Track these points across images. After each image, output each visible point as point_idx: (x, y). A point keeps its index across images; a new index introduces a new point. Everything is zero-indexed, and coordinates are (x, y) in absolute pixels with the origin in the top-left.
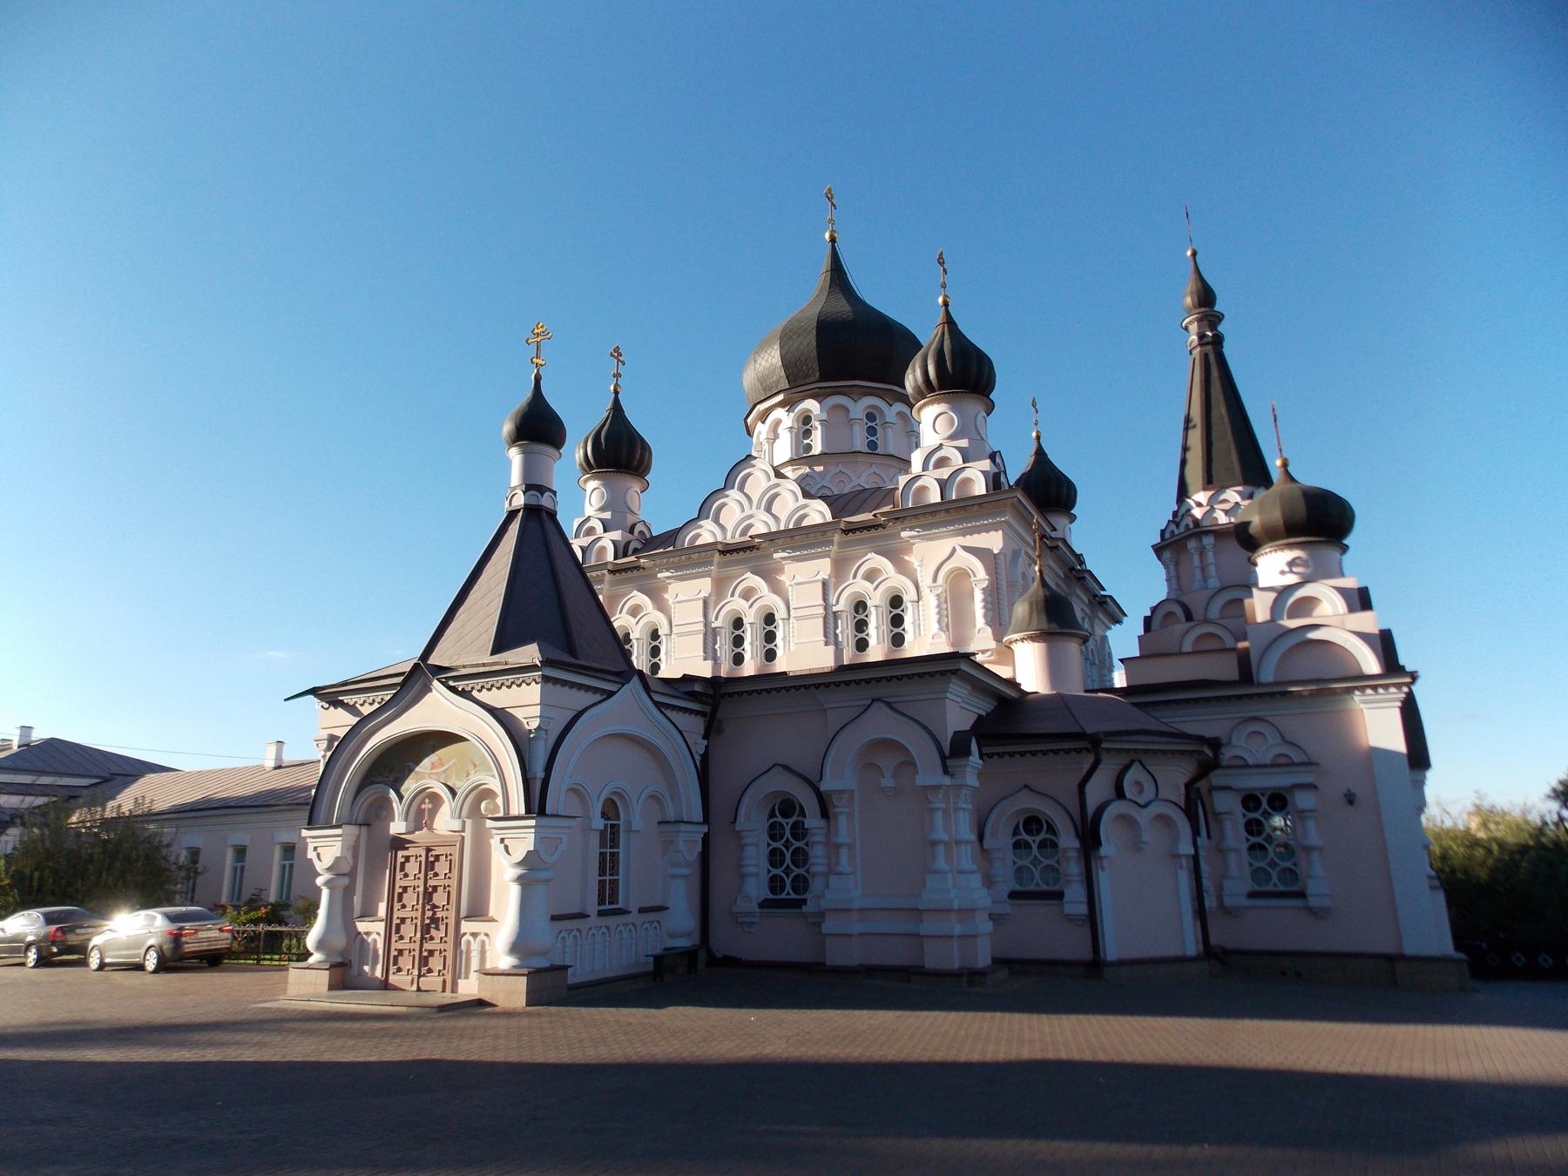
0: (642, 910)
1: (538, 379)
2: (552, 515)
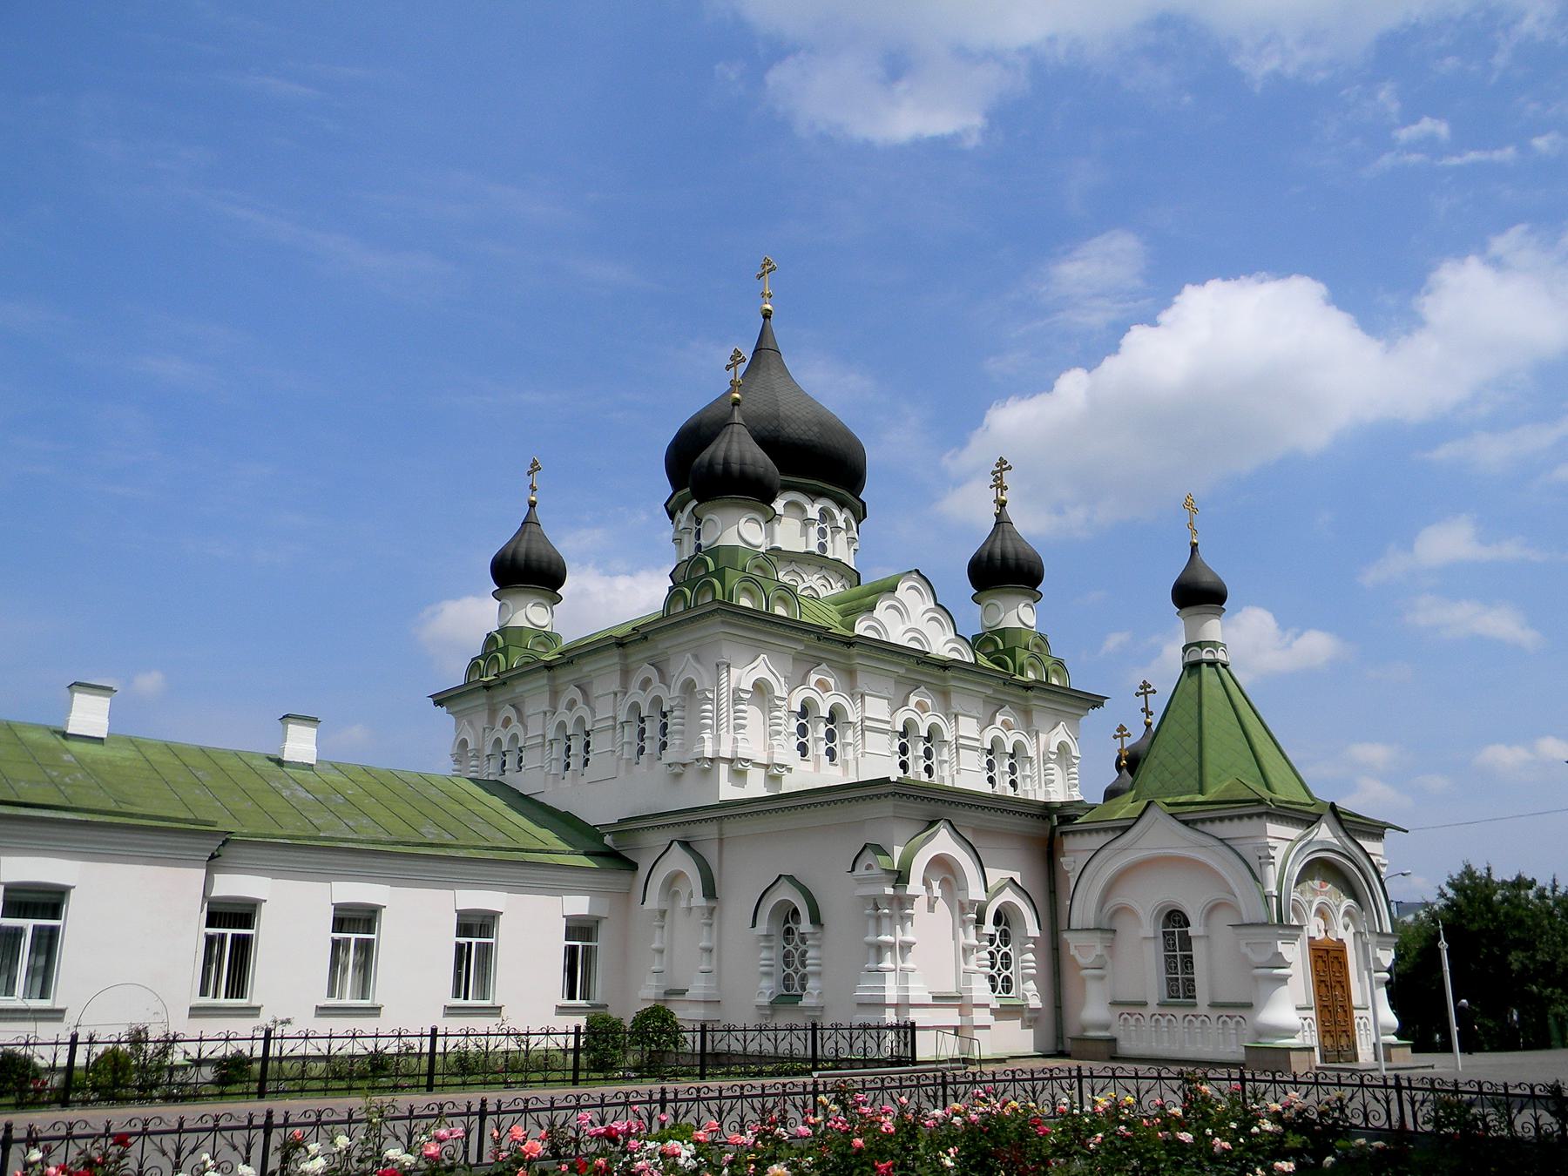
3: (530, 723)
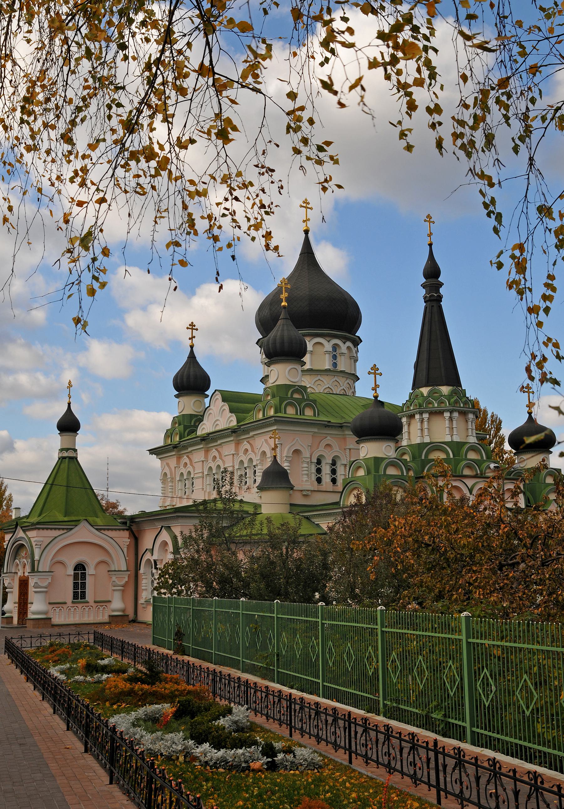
0: (95, 602)
1: (69, 404)
2: (74, 459)
3: (196, 465)
